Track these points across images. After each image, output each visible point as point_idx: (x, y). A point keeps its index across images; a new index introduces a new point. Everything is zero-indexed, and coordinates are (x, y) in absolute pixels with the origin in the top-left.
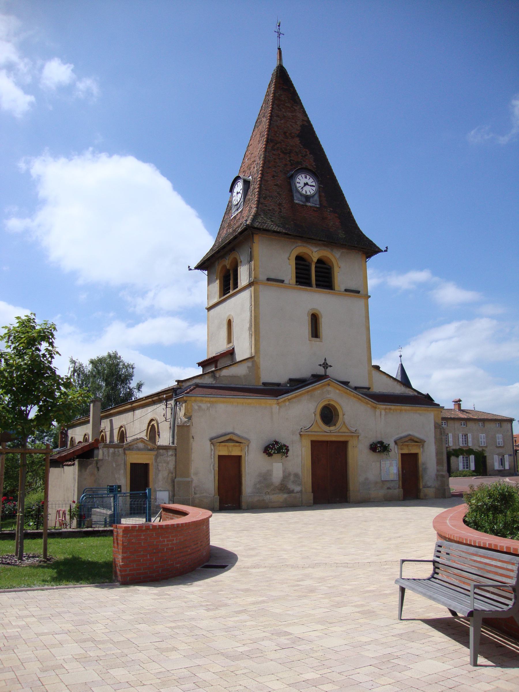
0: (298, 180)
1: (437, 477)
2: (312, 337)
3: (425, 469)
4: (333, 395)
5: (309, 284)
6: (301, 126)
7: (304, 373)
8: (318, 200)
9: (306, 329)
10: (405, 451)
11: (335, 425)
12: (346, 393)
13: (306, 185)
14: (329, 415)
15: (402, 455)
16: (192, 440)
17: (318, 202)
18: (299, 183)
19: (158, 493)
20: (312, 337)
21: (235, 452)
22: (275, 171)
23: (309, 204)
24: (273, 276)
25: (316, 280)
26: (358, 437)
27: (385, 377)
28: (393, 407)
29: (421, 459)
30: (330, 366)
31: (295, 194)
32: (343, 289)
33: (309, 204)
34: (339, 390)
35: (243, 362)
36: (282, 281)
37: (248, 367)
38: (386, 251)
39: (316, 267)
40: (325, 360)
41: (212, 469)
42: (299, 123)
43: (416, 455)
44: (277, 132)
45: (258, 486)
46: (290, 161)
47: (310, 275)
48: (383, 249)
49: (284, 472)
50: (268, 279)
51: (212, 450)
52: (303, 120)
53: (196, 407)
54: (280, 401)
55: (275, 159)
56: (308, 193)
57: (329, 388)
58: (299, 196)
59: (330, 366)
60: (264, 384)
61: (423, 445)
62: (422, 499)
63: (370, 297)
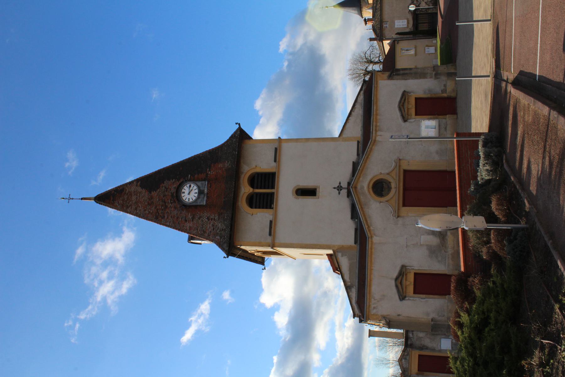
0: (187, 200)
1: (438, 78)
4: (365, 184)
5: (272, 194)
6: (142, 188)
7: (344, 204)
8: (201, 182)
9: (308, 201)
10: (413, 111)
11: (390, 182)
12: (363, 169)
13: (190, 193)
14: (380, 188)
15: (416, 115)
16: (401, 317)
17: (203, 182)
18: (189, 199)
19: (442, 348)
21: (411, 278)
23: (206, 191)
24: (268, 230)
25: (268, 188)
26: (400, 160)
28: (374, 123)
29: (421, 95)
30: (340, 183)
31: (199, 204)
32: (274, 164)
33: (206, 191)
34: (360, 177)
36: (271, 222)
37: (342, 256)
38: (239, 124)
39: (257, 188)
40: (335, 188)
41: (424, 300)
42: (139, 189)
43: (416, 99)
44: (149, 212)
45: (440, 259)
46: (172, 203)
47: (264, 194)
48: (237, 126)
50: (270, 234)
51: (409, 299)
52: (137, 185)
53: (375, 311)
54: (369, 235)
55: (171, 217)
56: (197, 191)
57: (359, 187)
58: (200, 199)
59: (340, 183)
60: (356, 243)
61: (408, 92)
62: (457, 95)
63: (279, 138)
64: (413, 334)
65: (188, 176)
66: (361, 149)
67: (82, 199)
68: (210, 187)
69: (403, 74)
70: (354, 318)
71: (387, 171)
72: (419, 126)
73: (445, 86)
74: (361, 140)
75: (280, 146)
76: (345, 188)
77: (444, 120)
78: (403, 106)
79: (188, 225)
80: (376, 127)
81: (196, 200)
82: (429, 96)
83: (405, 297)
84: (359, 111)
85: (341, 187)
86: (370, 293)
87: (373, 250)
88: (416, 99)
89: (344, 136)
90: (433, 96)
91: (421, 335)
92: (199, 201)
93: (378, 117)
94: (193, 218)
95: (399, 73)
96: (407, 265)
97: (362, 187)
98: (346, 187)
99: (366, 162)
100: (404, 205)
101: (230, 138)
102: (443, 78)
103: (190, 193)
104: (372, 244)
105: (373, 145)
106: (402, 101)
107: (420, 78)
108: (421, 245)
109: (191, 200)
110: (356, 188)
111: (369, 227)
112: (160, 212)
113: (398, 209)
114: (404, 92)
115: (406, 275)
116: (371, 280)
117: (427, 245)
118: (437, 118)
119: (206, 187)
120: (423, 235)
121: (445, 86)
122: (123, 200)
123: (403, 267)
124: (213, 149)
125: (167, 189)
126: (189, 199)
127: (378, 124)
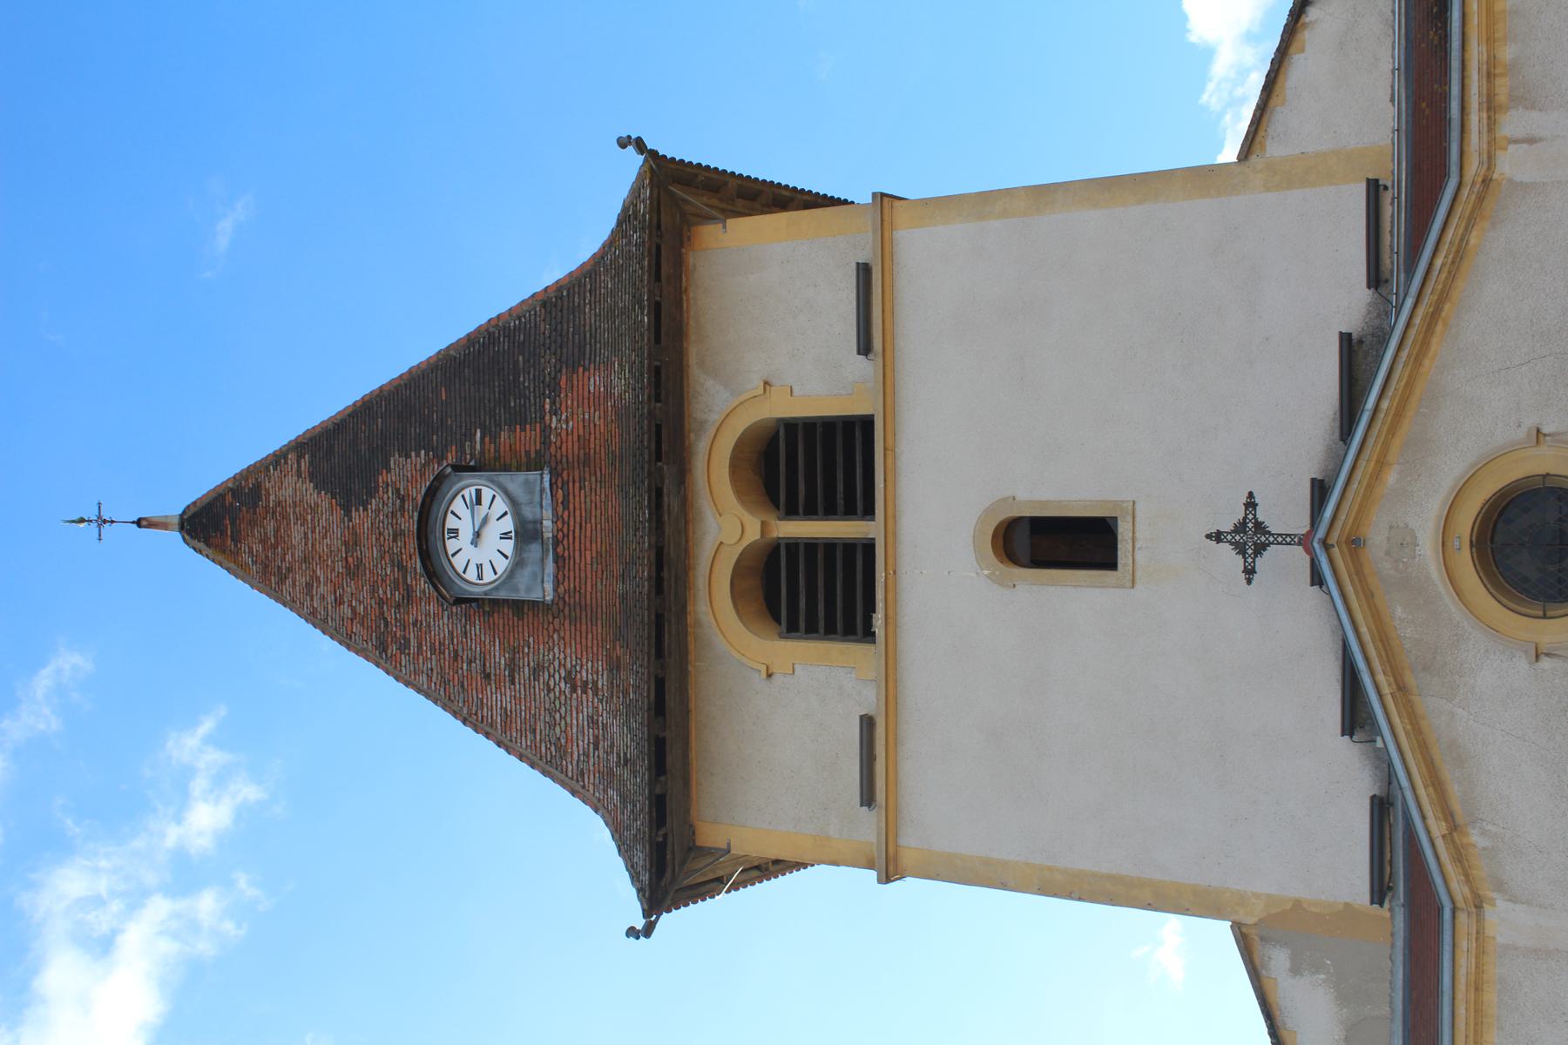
0: (471, 575)
2: (1111, 564)
8: (522, 476)
12: (1399, 414)
17: (533, 476)
18: (479, 567)
20: (1111, 564)
22: (470, 662)
23: (547, 524)
28: (1476, 53)
30: (1251, 504)
33: (547, 524)
34: (1382, 464)
35: (1271, 998)
36: (868, 723)
37: (1295, 970)
38: (640, 145)
47: (830, 546)
48: (635, 161)
50: (868, 799)
56: (508, 524)
57: (1377, 537)
60: (1380, 891)
65: (472, 439)
67: (139, 523)
68: (562, 505)
74: (1391, 168)
75: (885, 246)
76: (1286, 539)
79: (498, 699)
81: (511, 573)
85: (1260, 527)
87: (1490, 997)
89: (1274, 149)
92: (524, 578)
94: (513, 667)
97: (1404, 542)
98: (1301, 525)
101: (620, 223)
103: (482, 538)
104: (1481, 952)
109: (489, 576)
110: (1355, 544)
111: (1454, 827)
112: (391, 615)
119: (547, 501)
122: (263, 541)
124: (558, 286)
125: (403, 501)
126: (479, 567)
127: (1507, 53)
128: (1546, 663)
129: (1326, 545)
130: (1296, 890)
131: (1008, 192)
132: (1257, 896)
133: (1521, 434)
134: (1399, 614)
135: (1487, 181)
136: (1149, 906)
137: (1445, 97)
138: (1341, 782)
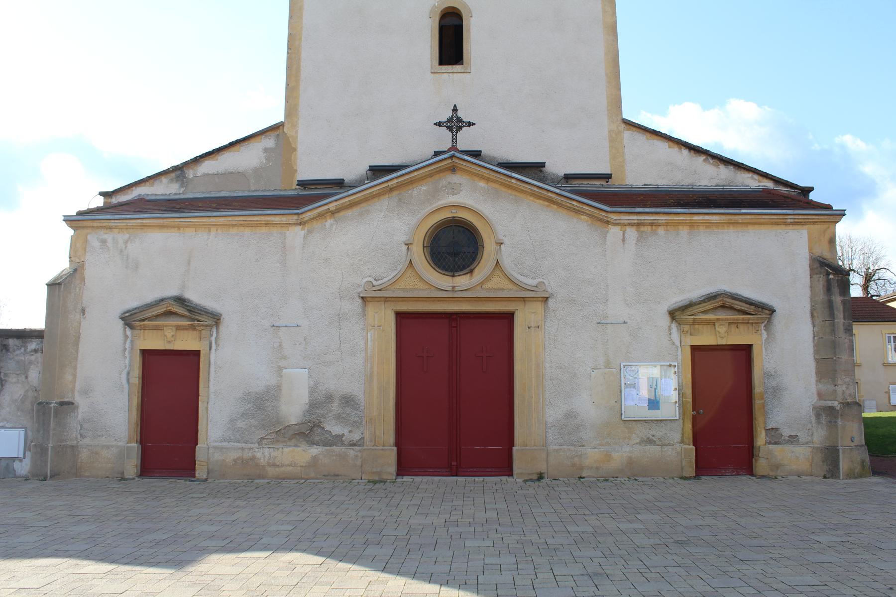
1: (818, 416)
2: (441, 63)
3: (777, 391)
9: (427, 43)
11: (471, 271)
12: (510, 187)
14: (455, 244)
15: (695, 349)
20: (441, 63)
21: (185, 342)
27: (663, 145)
28: (662, 218)
29: (762, 363)
30: (470, 124)
34: (488, 180)
35: (252, 140)
37: (266, 150)
41: (124, 382)
45: (241, 424)
49: (312, 391)
51: (126, 337)
54: (307, 216)
57: (456, 178)
60: (303, 184)
61: (769, 320)
62: (763, 477)
64: (36, 351)
66: (586, 185)
69: (830, 306)
70: (101, 194)
71: (507, 262)
72: (655, 359)
73: (793, 440)
74: (616, 184)
76: (454, 140)
77: (676, 436)
78: (723, 307)
80: (652, 224)
82: (758, 389)
83: (132, 327)
84: (710, 177)
85: (459, 128)
86: (143, 227)
87: (264, 230)
88: (747, 349)
89: (628, 135)
90: (757, 403)
91: (34, 375)
93: (684, 231)
95: (836, 290)
96: (222, 328)
97: (454, 189)
98: (461, 146)
99: (539, 197)
100: (401, 317)
102: (819, 436)
105: (590, 216)
106: (738, 305)
107: (817, 361)
108: (280, 369)
110: (453, 169)
111: (333, 213)
113: (386, 299)
114: (772, 311)
115: (193, 328)
116: (179, 227)
117: (279, 387)
118: (683, 414)
120: (310, 376)
121: (793, 439)
123: (216, 319)
127: (661, 231)
128: (405, 248)
129: (452, 157)
130: (301, 149)
131: (614, 14)
132: (296, 132)
133: (501, 237)
134: (422, 189)
135: (608, 222)
136: (287, 85)
137: (644, 206)
138: (351, 167)
